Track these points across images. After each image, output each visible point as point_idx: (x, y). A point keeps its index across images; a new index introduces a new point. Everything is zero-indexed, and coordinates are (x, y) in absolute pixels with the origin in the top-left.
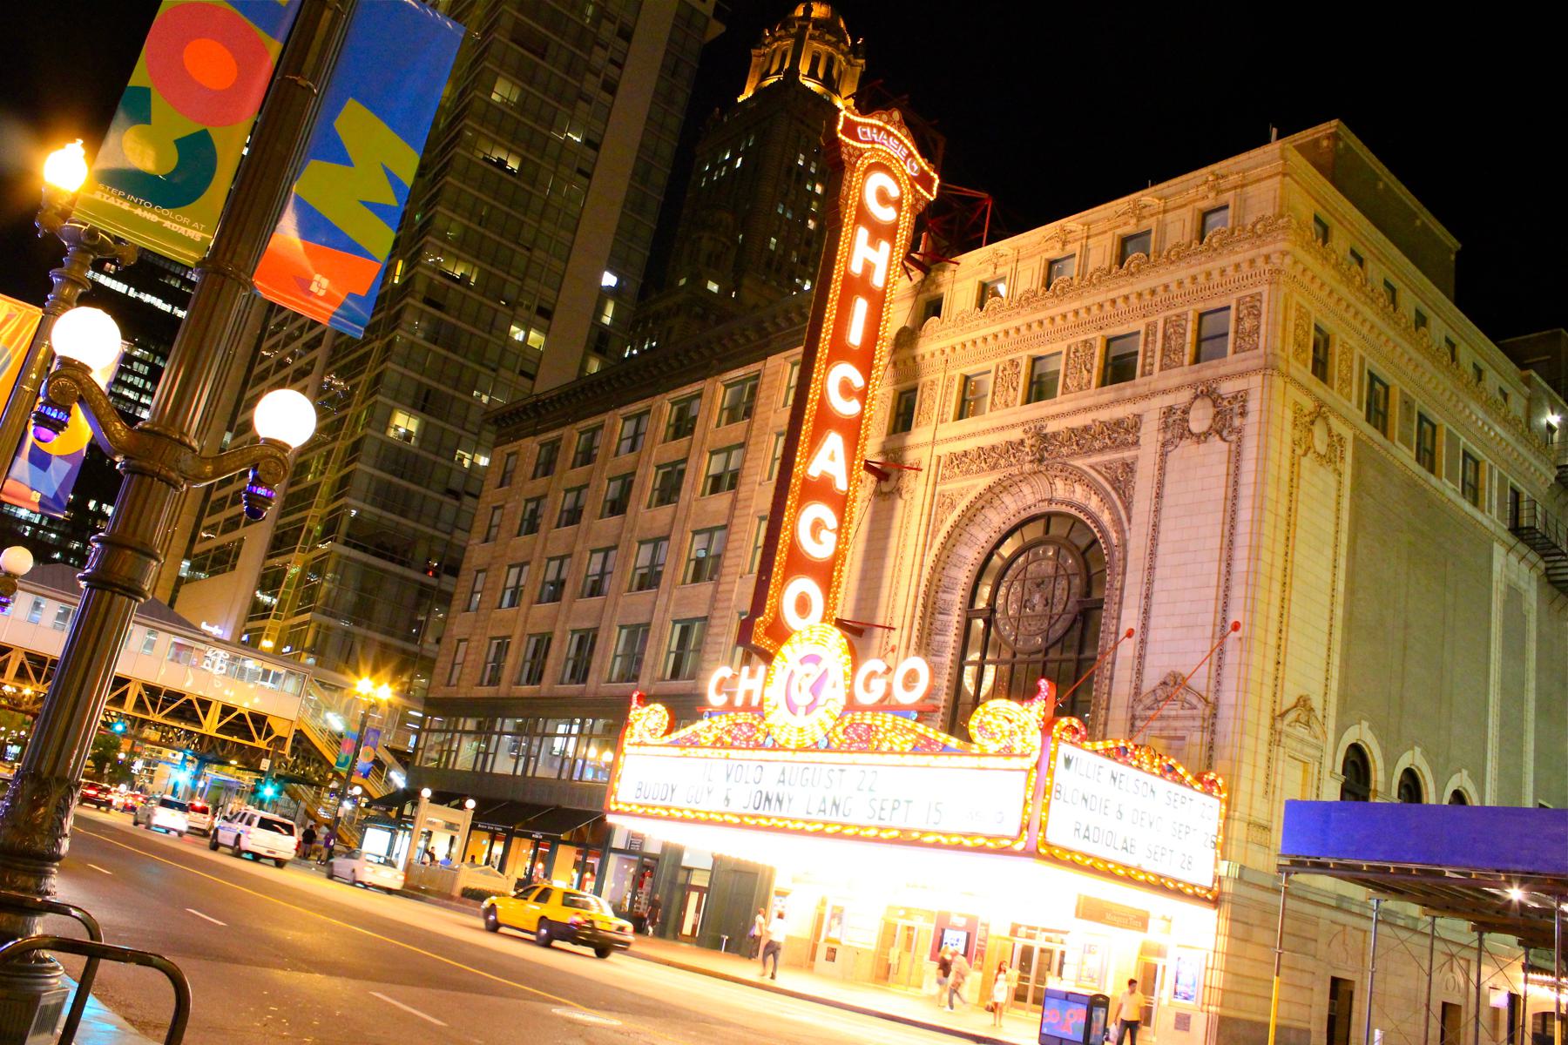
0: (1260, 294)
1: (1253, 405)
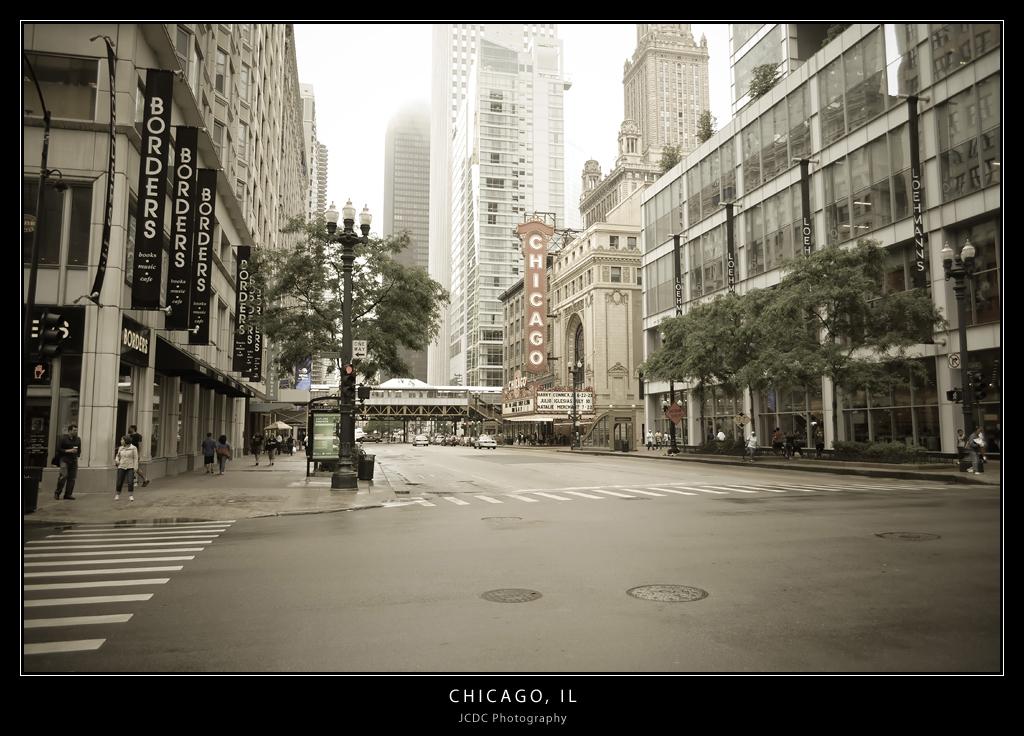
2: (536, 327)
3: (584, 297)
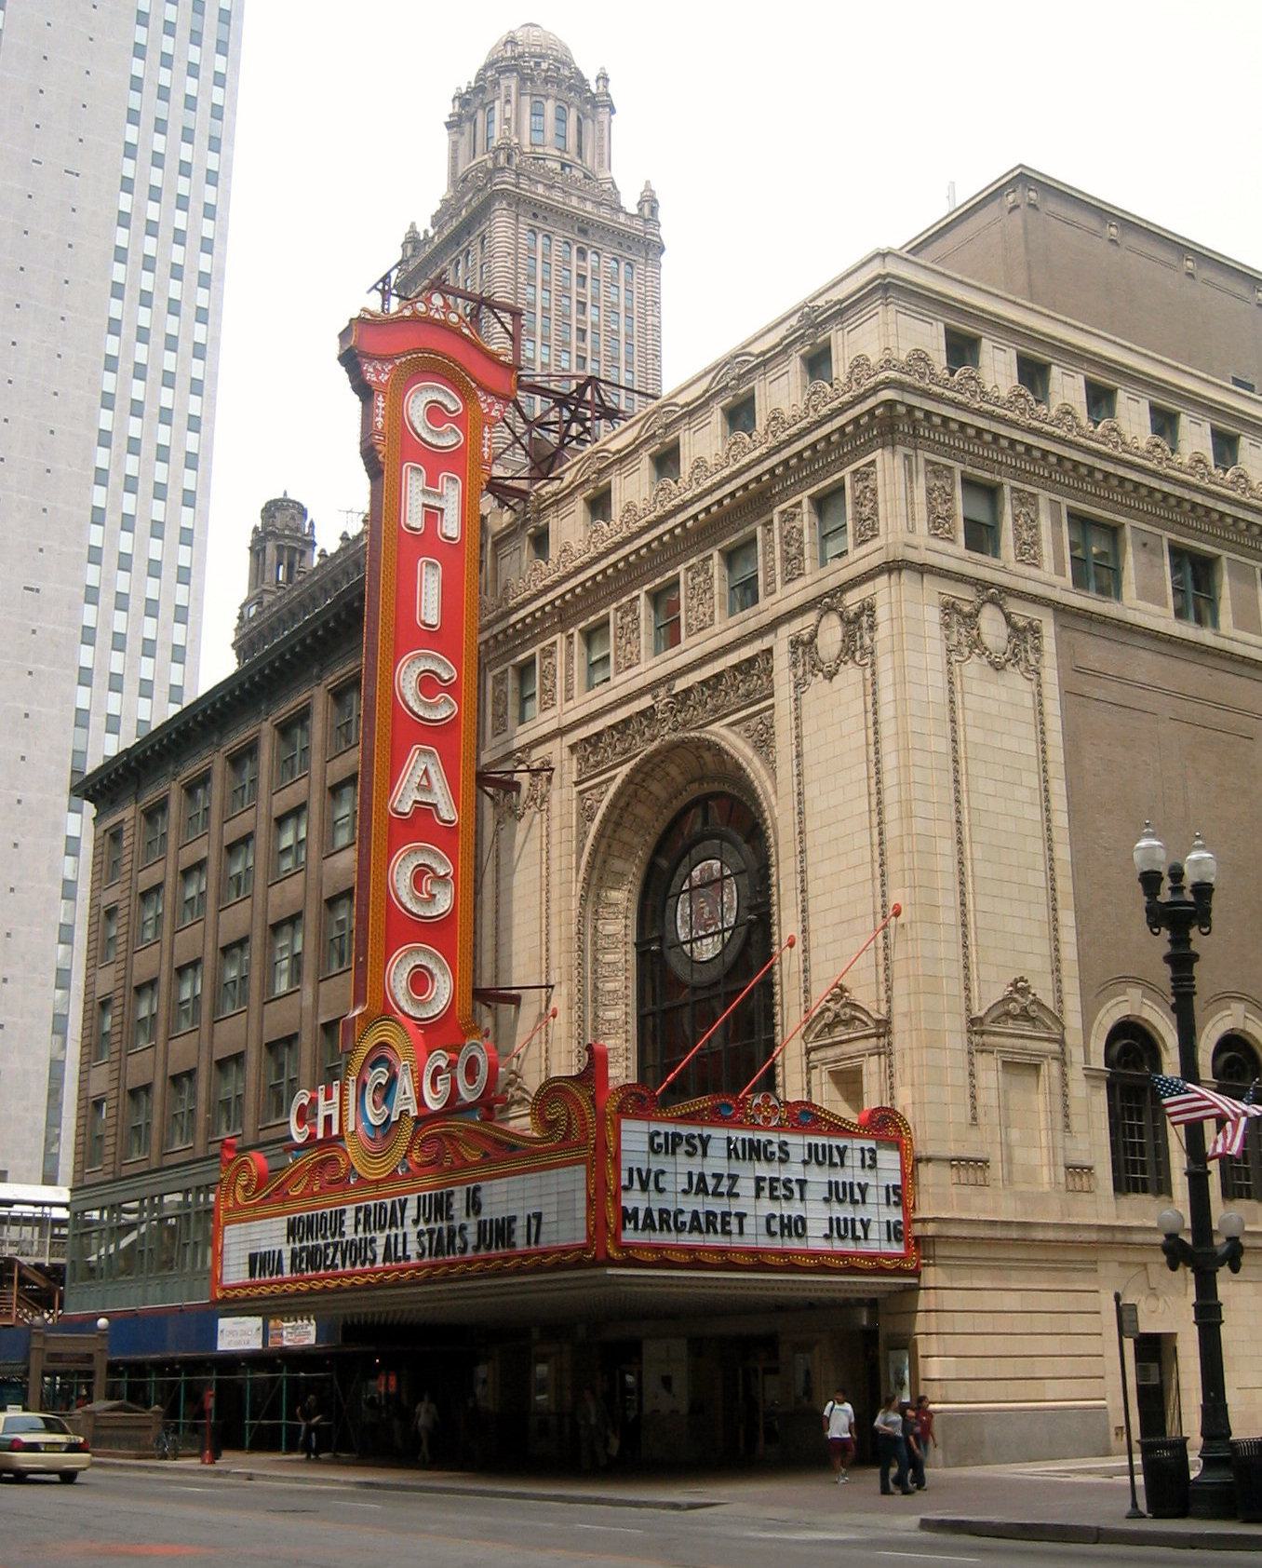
0: (872, 463)
1: (882, 614)
2: (421, 823)
3: (780, 643)
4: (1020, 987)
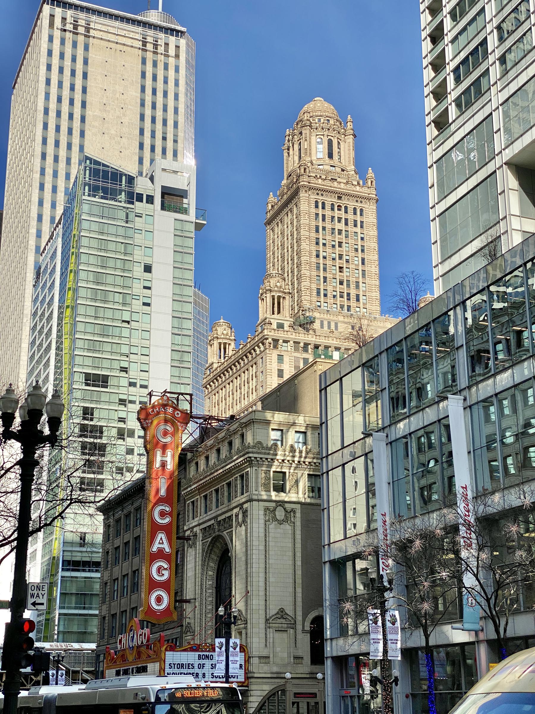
2: (160, 555)
4: (282, 610)
